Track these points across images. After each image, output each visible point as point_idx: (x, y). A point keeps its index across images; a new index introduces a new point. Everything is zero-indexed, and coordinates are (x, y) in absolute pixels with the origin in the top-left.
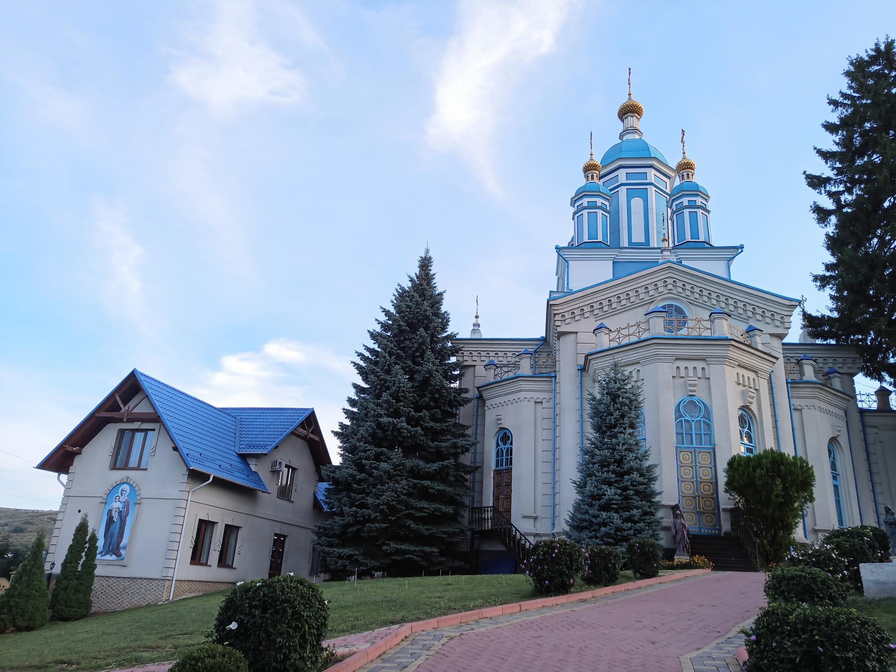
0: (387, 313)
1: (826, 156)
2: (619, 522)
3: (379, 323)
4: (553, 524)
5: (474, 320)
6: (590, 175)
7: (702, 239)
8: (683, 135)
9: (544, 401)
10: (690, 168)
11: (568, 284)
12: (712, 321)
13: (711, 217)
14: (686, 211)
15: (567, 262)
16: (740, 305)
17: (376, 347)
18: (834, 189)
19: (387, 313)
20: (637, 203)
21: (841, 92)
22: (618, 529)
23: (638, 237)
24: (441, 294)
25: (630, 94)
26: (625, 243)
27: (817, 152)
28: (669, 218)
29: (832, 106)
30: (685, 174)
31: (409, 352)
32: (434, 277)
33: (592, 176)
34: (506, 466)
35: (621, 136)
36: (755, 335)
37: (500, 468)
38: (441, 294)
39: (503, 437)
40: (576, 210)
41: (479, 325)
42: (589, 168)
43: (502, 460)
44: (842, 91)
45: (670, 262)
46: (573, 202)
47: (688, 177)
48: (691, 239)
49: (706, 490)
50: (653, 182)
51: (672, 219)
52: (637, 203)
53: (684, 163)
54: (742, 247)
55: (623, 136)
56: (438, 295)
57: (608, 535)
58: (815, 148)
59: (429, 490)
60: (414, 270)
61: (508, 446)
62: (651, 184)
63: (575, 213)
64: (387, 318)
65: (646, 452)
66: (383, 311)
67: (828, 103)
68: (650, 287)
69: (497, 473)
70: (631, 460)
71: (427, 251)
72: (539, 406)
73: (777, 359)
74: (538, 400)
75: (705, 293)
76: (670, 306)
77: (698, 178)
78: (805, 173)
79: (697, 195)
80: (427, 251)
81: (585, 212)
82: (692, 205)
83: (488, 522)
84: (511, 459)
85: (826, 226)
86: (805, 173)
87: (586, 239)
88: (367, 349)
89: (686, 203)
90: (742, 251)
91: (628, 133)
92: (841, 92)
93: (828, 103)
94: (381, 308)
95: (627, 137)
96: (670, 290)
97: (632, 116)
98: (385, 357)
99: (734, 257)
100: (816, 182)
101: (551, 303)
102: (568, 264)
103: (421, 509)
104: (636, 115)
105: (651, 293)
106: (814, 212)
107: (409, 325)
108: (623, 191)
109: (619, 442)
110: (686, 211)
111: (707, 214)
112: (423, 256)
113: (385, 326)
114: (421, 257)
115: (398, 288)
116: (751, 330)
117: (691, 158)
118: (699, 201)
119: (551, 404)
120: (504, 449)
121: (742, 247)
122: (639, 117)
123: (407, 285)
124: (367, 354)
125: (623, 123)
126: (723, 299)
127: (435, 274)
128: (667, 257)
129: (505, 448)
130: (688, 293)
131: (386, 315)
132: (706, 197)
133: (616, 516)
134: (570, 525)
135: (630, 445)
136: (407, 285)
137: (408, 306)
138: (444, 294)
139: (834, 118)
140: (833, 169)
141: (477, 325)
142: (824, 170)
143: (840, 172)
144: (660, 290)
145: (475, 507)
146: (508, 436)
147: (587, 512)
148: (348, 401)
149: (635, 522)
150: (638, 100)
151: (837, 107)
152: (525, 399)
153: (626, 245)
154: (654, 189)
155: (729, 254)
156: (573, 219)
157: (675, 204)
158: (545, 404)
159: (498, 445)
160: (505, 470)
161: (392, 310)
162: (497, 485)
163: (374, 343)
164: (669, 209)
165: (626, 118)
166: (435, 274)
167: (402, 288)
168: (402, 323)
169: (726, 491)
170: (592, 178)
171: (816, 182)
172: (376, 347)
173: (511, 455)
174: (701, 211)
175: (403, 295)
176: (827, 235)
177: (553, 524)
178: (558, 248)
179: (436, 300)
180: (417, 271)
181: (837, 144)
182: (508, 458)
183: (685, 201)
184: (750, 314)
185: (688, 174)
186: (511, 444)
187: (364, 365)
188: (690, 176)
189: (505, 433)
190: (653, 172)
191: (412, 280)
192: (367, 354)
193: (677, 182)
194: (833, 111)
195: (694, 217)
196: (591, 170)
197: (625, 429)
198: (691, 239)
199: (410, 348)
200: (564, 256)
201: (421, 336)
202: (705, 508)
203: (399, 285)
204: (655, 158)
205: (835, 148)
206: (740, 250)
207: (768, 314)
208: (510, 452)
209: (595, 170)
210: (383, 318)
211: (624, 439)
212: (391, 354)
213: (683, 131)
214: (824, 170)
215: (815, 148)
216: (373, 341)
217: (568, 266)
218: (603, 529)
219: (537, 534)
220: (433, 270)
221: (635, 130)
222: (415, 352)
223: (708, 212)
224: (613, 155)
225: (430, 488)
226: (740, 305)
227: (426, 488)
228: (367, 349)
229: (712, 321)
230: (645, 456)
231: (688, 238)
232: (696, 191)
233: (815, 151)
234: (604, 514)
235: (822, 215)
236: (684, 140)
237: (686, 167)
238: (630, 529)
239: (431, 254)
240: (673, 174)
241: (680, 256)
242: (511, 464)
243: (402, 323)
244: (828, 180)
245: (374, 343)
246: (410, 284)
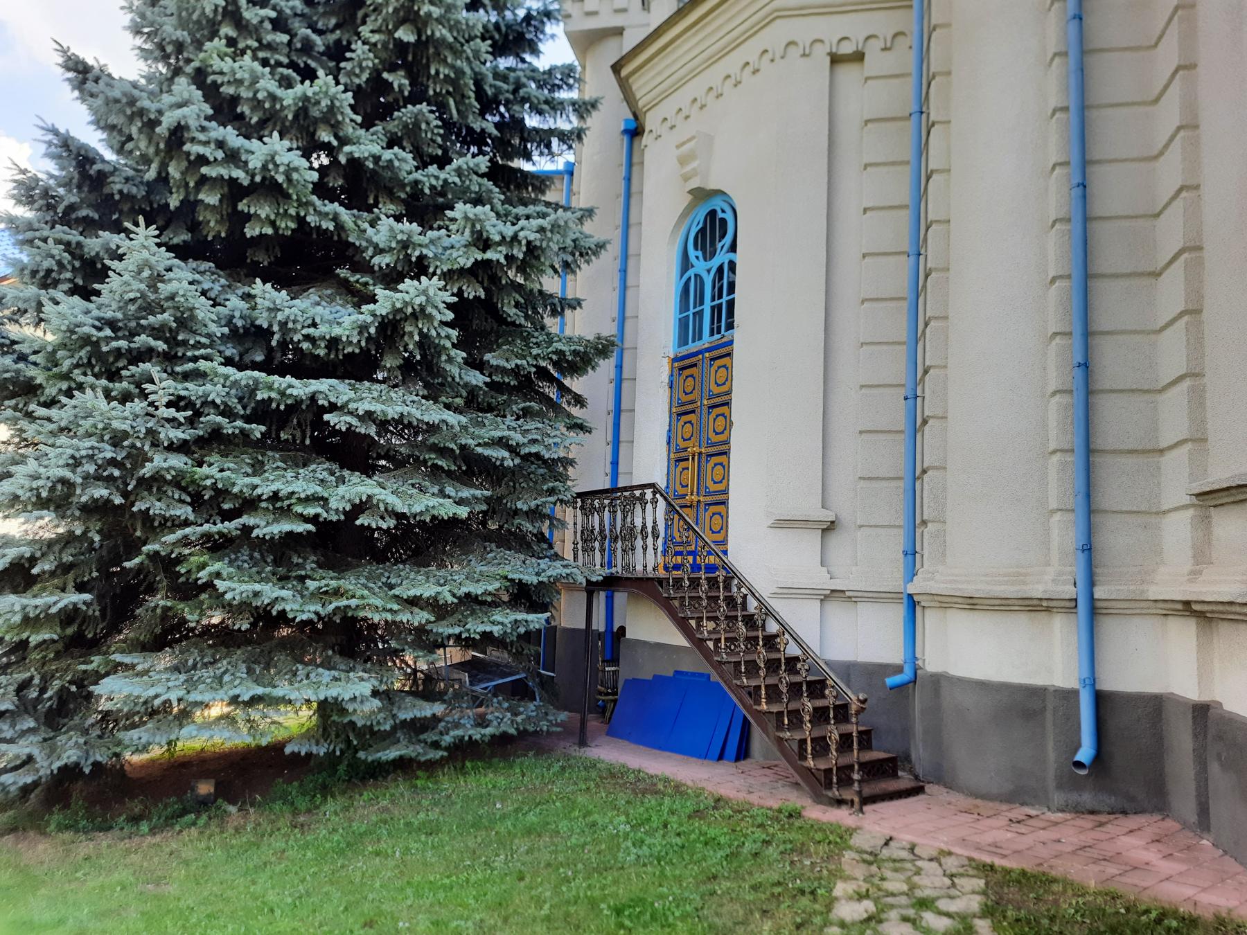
4: (911, 553)
9: (873, 52)
34: (712, 334)
37: (692, 347)
39: (702, 231)
43: (700, 314)
59: (326, 417)
61: (721, 258)
69: (683, 365)
72: (848, 73)
74: (847, 48)
83: (645, 549)
84: (731, 304)
103: (279, 505)
119: (904, 57)
120: (704, 275)
129: (709, 271)
145: (620, 485)
146: (723, 222)
152: (792, 49)
158: (875, 61)
159: (686, 264)
160: (708, 350)
162: (682, 411)
177: (911, 553)
182: (720, 306)
186: (733, 248)
189: (712, 213)
208: (725, 280)
219: (833, 591)
225: (333, 408)
227: (315, 409)
242: (730, 326)
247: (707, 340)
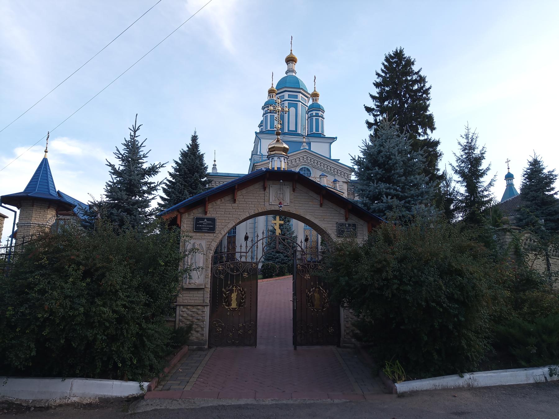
0: (177, 163)
1: (373, 97)
2: (283, 257)
3: (173, 168)
5: (213, 163)
6: (272, 95)
7: (320, 132)
8: (315, 79)
10: (317, 96)
11: (260, 150)
12: (320, 178)
13: (325, 120)
14: (314, 118)
15: (260, 140)
16: (332, 169)
17: (171, 179)
18: (375, 113)
19: (177, 163)
20: (292, 110)
21: (382, 69)
22: (283, 260)
23: (292, 128)
24: (202, 155)
25: (291, 50)
26: (286, 130)
27: (370, 96)
28: (306, 119)
29: (377, 76)
30: (315, 99)
31: (189, 183)
32: (199, 145)
33: (273, 96)
35: (286, 73)
36: (336, 183)
38: (202, 155)
40: (264, 113)
41: (216, 165)
42: (271, 92)
44: (382, 68)
45: (306, 149)
46: (263, 108)
47: (316, 101)
48: (316, 131)
49: (314, 244)
50: (300, 100)
51: (308, 120)
52: (292, 110)
53: (315, 93)
54: (336, 138)
55: (287, 73)
56: (201, 155)
57: (279, 262)
58: (370, 94)
60: (189, 142)
62: (299, 101)
63: (264, 114)
64: (177, 165)
65: (293, 231)
66: (174, 162)
67: (376, 74)
68: (297, 160)
70: (288, 235)
71: (195, 132)
73: (344, 193)
75: (319, 163)
76: (305, 168)
77: (320, 102)
78: (364, 105)
79: (319, 111)
80: (195, 132)
81: (269, 115)
82: (317, 115)
84: (235, 231)
85: (371, 130)
86: (364, 105)
87: (269, 129)
88: (168, 180)
89: (314, 114)
90: (336, 140)
91: (290, 72)
92: (382, 69)
93: (376, 74)
94: (174, 160)
95: (289, 74)
96: (305, 161)
97: (292, 63)
98: (179, 186)
99: (332, 143)
100: (368, 110)
101: (255, 164)
102: (261, 141)
104: (294, 62)
105: (297, 162)
106: (366, 124)
107: (189, 170)
108: (286, 103)
109: (284, 228)
110: (314, 118)
111: (323, 120)
112: (193, 135)
113: (176, 170)
114: (192, 135)
115: (182, 151)
116: (335, 181)
117: (318, 91)
118: (320, 113)
121: (336, 138)
122: (295, 63)
123: (186, 149)
124: (168, 183)
125: (288, 65)
126: (326, 166)
127: (199, 144)
128: (304, 146)
130: (312, 163)
131: (176, 164)
132: (323, 112)
133: (282, 255)
134: (264, 259)
135: (288, 229)
136: (186, 149)
137: (188, 161)
138: (204, 155)
139: (379, 80)
140: (376, 105)
141: (215, 165)
142: (372, 104)
143: (378, 106)
144: (301, 161)
147: (271, 254)
148: (158, 204)
149: (288, 257)
150: (296, 54)
151: (379, 77)
153: (287, 131)
154: (300, 103)
155: (330, 141)
156: (263, 116)
157: (309, 113)
161: (180, 162)
163: (171, 178)
164: (307, 115)
165: (289, 63)
166: (199, 144)
167: (184, 151)
168: (186, 170)
169: (321, 245)
170: (273, 97)
171: (368, 110)
172: (171, 179)
173: (235, 229)
174: (321, 118)
175: (184, 155)
176: (371, 134)
178: (256, 133)
179: (201, 157)
180: (191, 142)
181: (378, 93)
183: (314, 113)
184: (336, 173)
185: (316, 99)
187: (167, 188)
188: (317, 100)
190: (301, 95)
191: (188, 147)
192: (168, 183)
193: (311, 102)
194: (377, 78)
195: (317, 121)
196: (272, 92)
197: (286, 223)
198: (316, 131)
199: (190, 182)
200: (259, 137)
201: (195, 176)
202: (313, 251)
203: (182, 150)
204: (302, 89)
205: (377, 95)
206: (335, 139)
207: (343, 173)
209: (274, 93)
210: (175, 165)
211: (286, 227)
212: (181, 184)
213: (315, 77)
214: (372, 104)
215: (370, 94)
216: (170, 176)
217: (260, 142)
218: (277, 260)
220: (199, 141)
221: (293, 71)
222: (192, 183)
223: (324, 118)
224: (283, 83)
226: (332, 169)
228: (168, 180)
229: (320, 178)
230: (293, 233)
231: (314, 131)
232: (319, 108)
233: (369, 95)
234: (278, 254)
235: (370, 125)
236: (315, 81)
237: (315, 95)
238: (287, 260)
239: (197, 134)
240: (309, 96)
241: (310, 140)
242: (235, 233)
243: (186, 170)
244: (373, 109)
245: (171, 178)
246: (187, 149)
247: (232, 235)
